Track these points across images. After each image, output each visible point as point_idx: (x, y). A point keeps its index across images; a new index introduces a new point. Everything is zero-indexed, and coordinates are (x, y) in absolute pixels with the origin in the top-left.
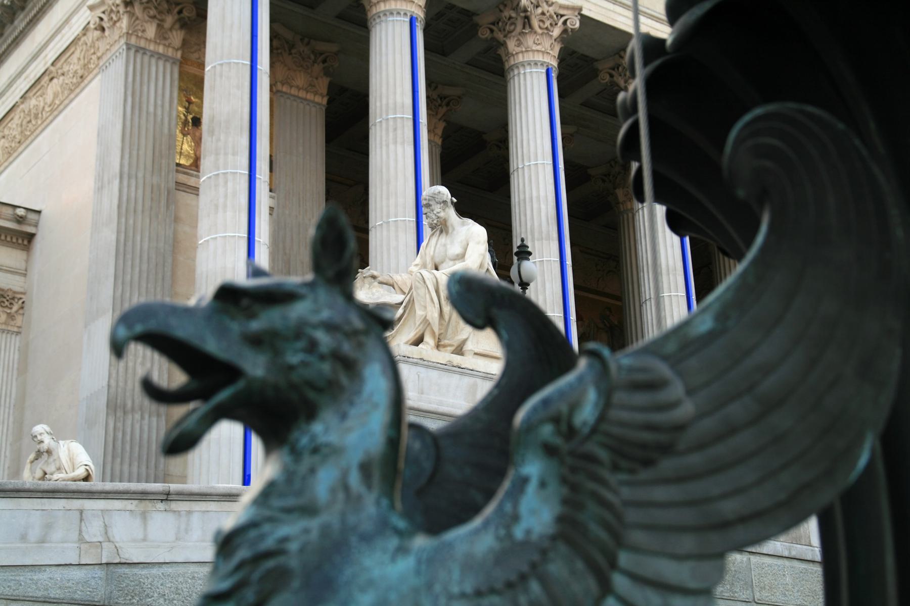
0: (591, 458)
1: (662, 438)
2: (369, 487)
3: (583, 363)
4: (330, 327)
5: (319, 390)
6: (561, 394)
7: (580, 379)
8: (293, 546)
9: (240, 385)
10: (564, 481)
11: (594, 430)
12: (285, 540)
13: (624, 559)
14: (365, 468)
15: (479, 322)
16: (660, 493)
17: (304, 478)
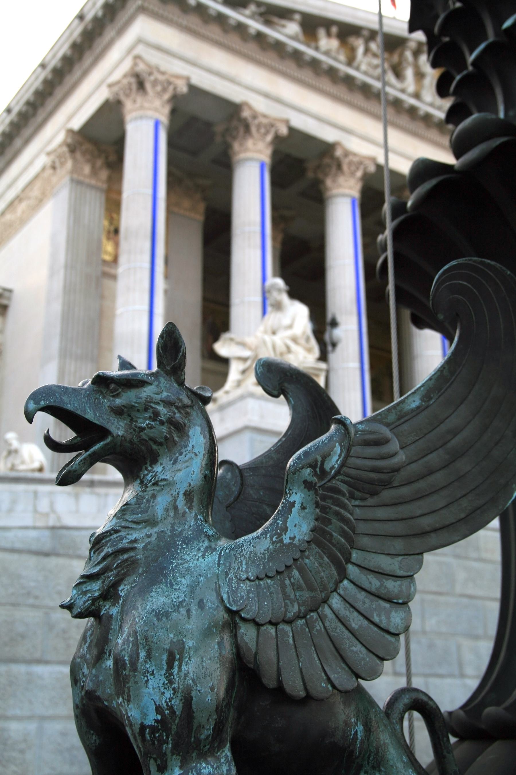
0: (337, 491)
1: (383, 476)
2: (190, 508)
3: (333, 427)
4: (167, 403)
5: (161, 444)
6: (317, 448)
7: (331, 438)
8: (140, 546)
9: (109, 440)
10: (317, 505)
11: (338, 473)
12: (135, 541)
13: (355, 555)
14: (188, 495)
15: (276, 393)
16: (381, 513)
17: (148, 501)
